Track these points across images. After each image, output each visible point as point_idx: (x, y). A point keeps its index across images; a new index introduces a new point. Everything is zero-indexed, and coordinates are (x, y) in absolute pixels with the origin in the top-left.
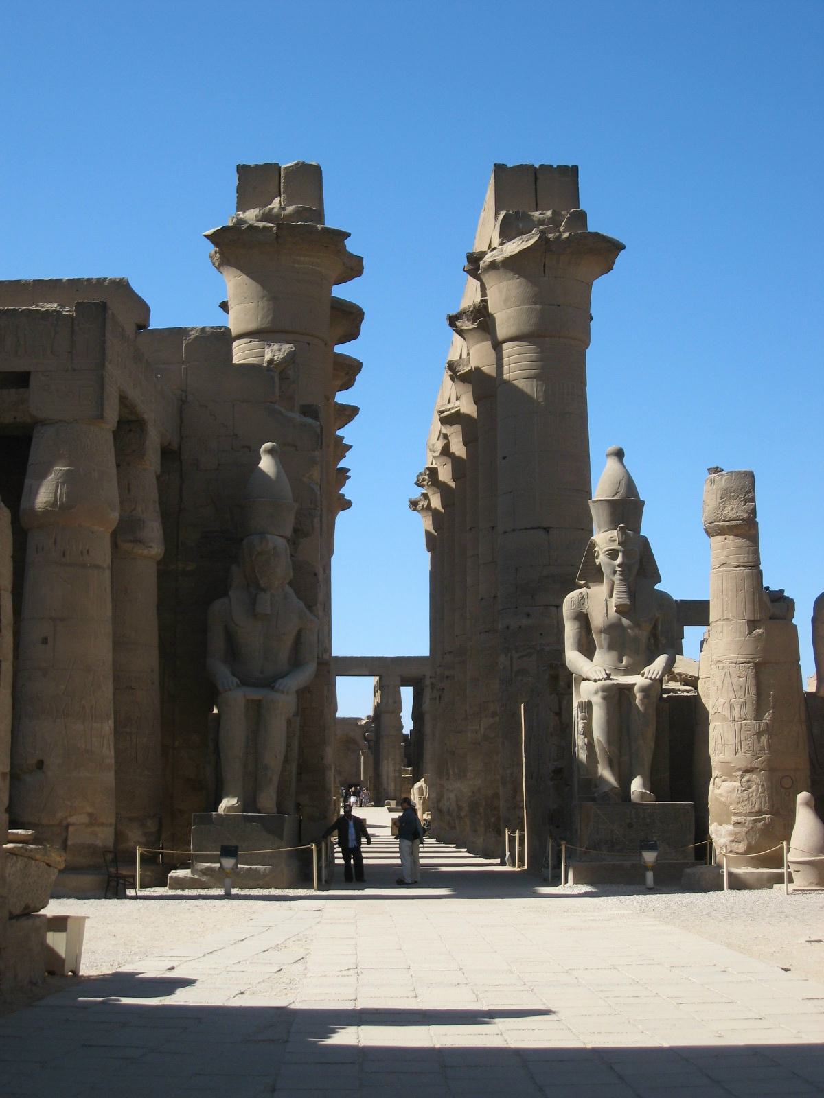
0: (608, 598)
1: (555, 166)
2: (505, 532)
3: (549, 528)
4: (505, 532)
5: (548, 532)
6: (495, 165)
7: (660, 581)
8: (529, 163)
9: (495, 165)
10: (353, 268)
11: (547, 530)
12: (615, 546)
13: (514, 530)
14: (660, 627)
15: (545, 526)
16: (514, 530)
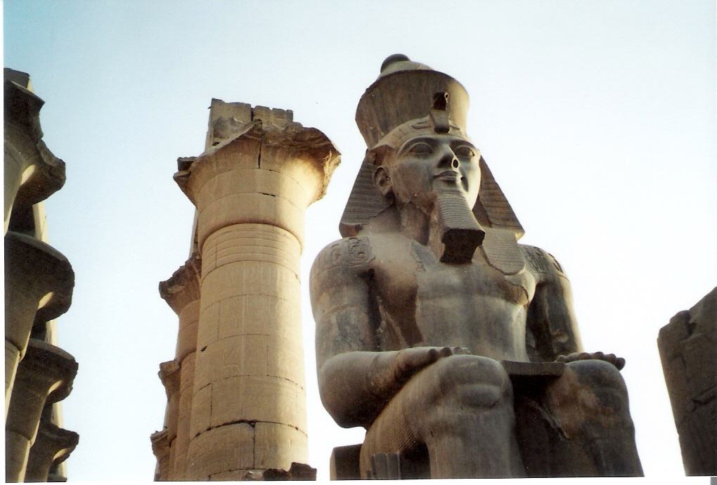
0: (417, 243)
1: (271, 109)
2: (198, 435)
3: (255, 422)
4: (198, 435)
5: (254, 426)
6: (213, 100)
7: (519, 228)
8: (246, 102)
9: (213, 100)
10: (51, 177)
11: (252, 423)
12: (429, 134)
13: (209, 429)
14: (547, 309)
15: (249, 420)
16: (209, 429)
